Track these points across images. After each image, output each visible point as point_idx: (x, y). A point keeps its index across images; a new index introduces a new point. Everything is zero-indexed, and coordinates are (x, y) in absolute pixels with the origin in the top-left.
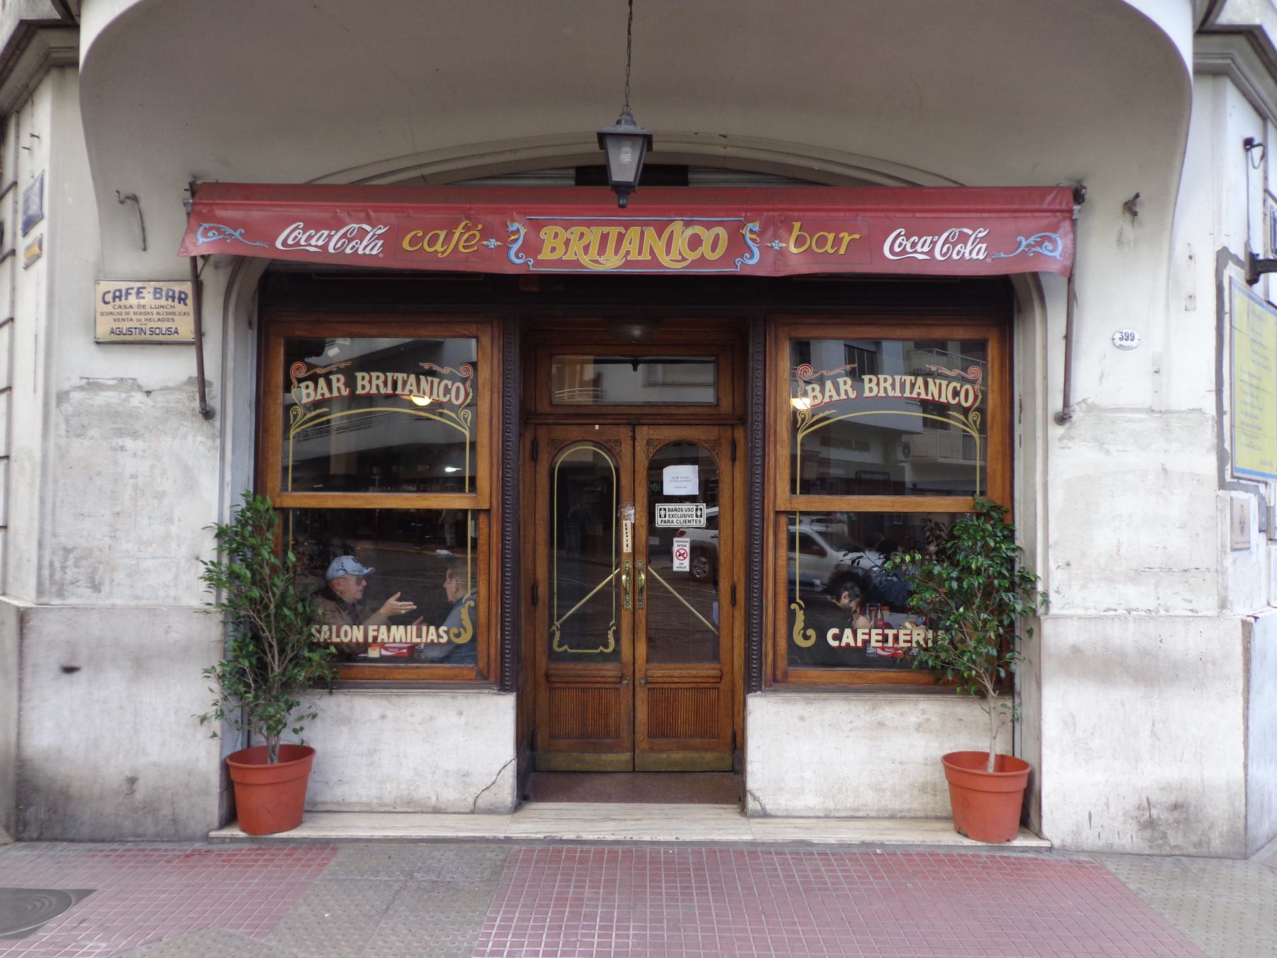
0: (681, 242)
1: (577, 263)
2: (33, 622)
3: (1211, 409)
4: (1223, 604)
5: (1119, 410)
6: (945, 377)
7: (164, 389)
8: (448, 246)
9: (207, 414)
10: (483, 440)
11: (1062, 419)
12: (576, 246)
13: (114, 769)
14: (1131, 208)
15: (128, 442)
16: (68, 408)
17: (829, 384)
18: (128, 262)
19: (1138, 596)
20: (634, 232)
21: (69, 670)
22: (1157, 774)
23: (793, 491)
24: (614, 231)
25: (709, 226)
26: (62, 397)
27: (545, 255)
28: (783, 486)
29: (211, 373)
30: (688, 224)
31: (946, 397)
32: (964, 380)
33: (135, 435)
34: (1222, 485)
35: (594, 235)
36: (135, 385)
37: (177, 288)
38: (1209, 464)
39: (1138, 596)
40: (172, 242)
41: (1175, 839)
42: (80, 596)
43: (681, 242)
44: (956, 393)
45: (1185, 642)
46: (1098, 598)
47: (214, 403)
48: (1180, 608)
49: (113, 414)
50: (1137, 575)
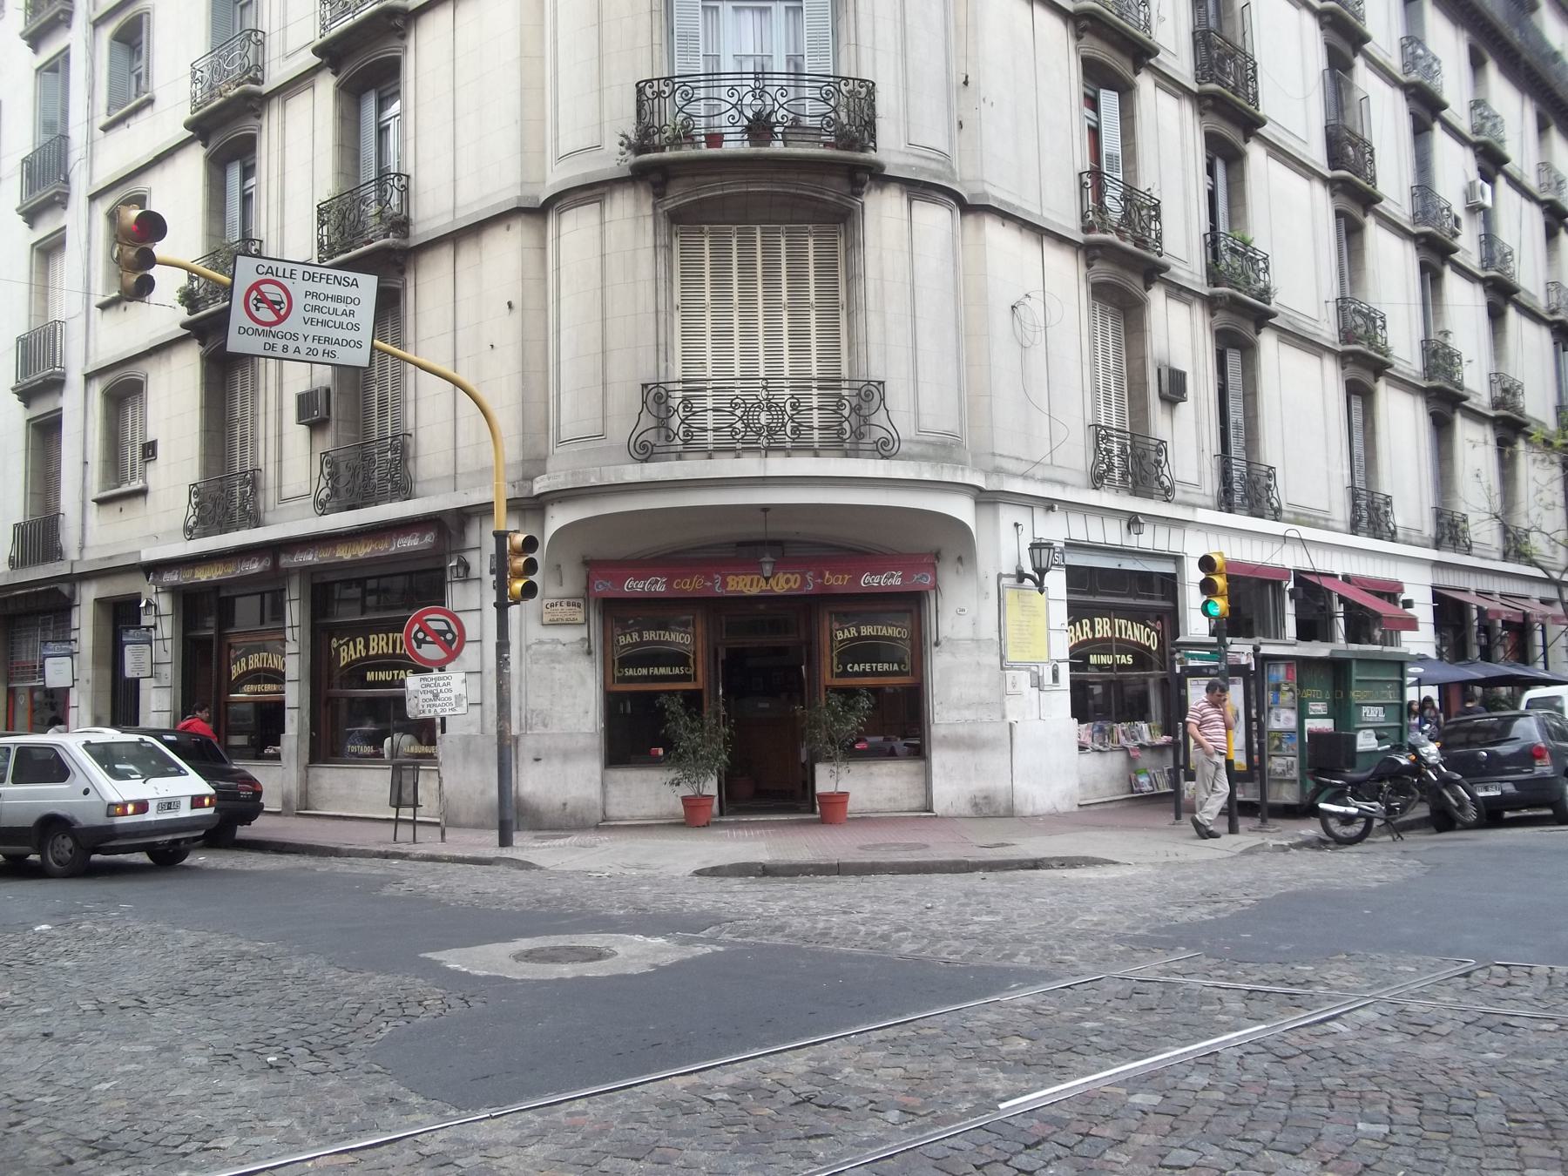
0: (782, 581)
2: (522, 741)
4: (1004, 717)
8: (691, 585)
10: (699, 659)
13: (558, 800)
14: (960, 559)
19: (968, 715)
21: (537, 760)
22: (977, 785)
26: (528, 648)
28: (828, 676)
31: (896, 634)
35: (748, 579)
36: (558, 642)
39: (968, 715)
41: (986, 811)
42: (539, 729)
43: (782, 581)
45: (987, 732)
46: (954, 716)
49: (549, 654)
50: (968, 706)
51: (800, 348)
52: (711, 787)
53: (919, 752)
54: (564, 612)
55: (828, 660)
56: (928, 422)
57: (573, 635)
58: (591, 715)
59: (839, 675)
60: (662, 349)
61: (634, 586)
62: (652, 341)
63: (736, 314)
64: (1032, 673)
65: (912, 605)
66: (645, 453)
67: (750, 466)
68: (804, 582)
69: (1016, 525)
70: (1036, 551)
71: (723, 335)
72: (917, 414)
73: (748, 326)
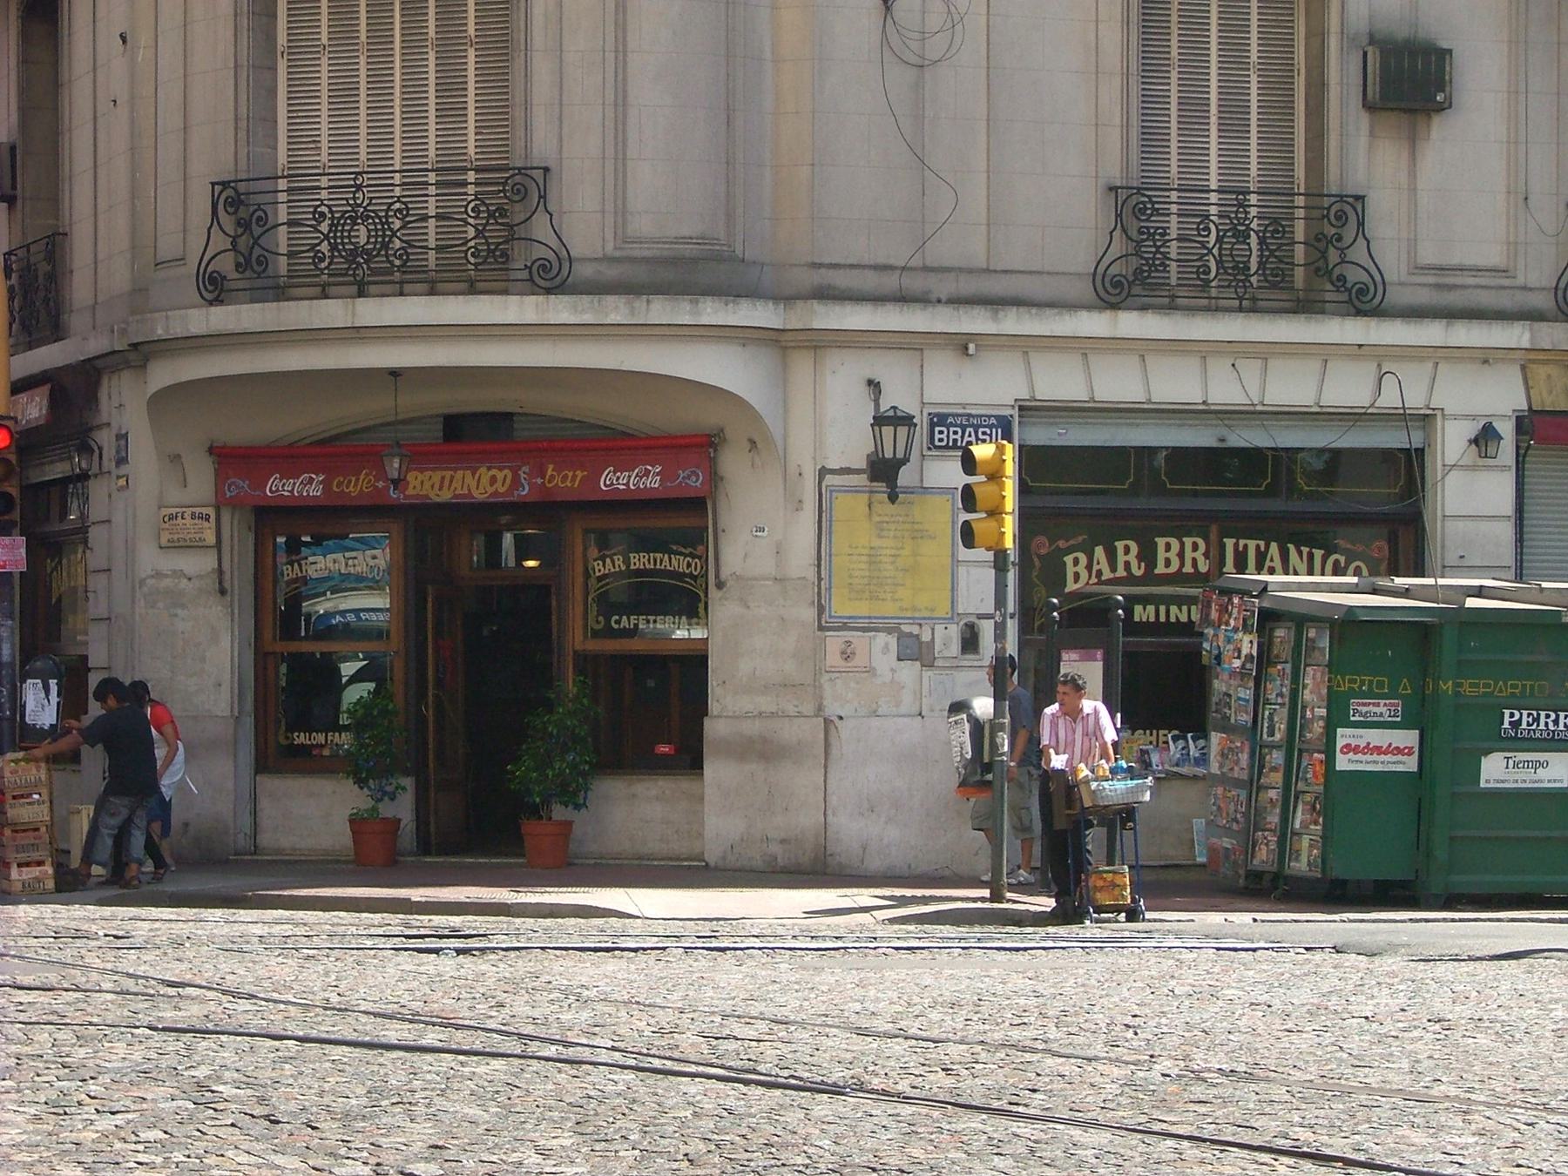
0: (485, 480)
1: (427, 496)
3: (811, 574)
5: (755, 579)
6: (681, 554)
7: (200, 577)
9: (223, 592)
11: (720, 585)
12: (427, 485)
15: (179, 611)
16: (145, 589)
17: (608, 561)
18: (175, 495)
19: (766, 703)
20: (460, 473)
23: (585, 637)
24: (448, 474)
25: (501, 469)
27: (410, 491)
29: (226, 566)
30: (489, 469)
31: (683, 568)
32: (693, 556)
33: (183, 606)
34: (821, 628)
35: (437, 477)
37: (205, 511)
38: (810, 614)
40: (201, 481)
44: (689, 565)
45: (790, 732)
46: (746, 704)
47: (227, 585)
48: (791, 710)
50: (766, 689)
51: (451, 111)
52: (403, 809)
53: (690, 759)
54: (188, 526)
55: (579, 609)
56: (642, 225)
57: (201, 564)
58: (226, 687)
59: (596, 634)
60: (257, 119)
61: (280, 487)
62: (231, 116)
63: (363, 60)
64: (902, 636)
65: (686, 519)
66: (215, 289)
67: (333, 312)
68: (516, 483)
69: (870, 382)
70: (888, 431)
71: (344, 94)
72: (622, 213)
73: (379, 80)
